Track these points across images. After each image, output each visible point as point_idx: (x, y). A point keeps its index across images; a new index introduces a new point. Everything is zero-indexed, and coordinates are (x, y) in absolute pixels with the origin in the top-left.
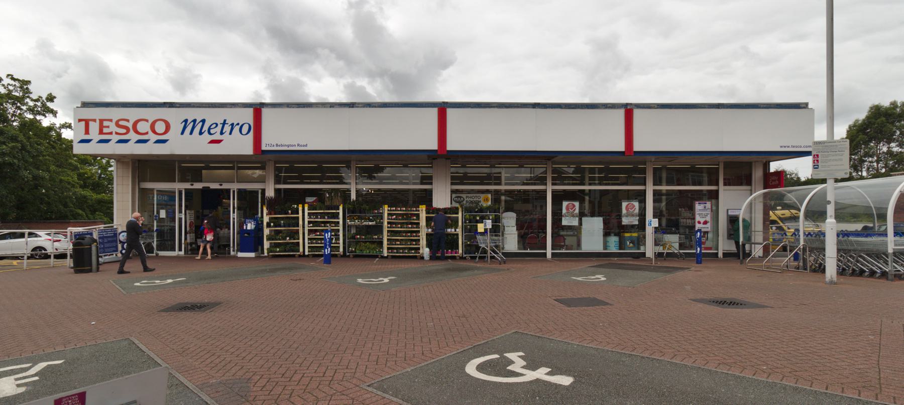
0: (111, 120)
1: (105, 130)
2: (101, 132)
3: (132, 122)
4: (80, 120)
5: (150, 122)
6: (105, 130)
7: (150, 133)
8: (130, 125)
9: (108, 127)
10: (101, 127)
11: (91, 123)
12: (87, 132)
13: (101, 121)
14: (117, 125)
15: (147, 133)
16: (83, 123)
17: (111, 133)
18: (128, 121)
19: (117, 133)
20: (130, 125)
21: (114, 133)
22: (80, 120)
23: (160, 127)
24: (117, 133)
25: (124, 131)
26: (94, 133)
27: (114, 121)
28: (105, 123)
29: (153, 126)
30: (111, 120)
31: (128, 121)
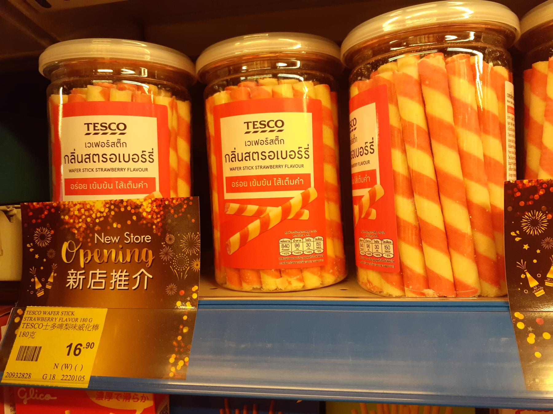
0: (257, 122)
1: (256, 127)
2: (254, 128)
3: (267, 122)
4: (245, 123)
5: (275, 121)
6: (256, 127)
7: (275, 127)
8: (266, 123)
9: (256, 125)
10: (254, 125)
11: (249, 123)
12: (248, 128)
13: (254, 122)
14: (260, 124)
15: (273, 127)
16: (246, 124)
17: (258, 128)
18: (265, 121)
19: (260, 128)
20: (266, 123)
21: (259, 127)
22: (245, 123)
23: (280, 124)
24: (260, 128)
25: (263, 126)
26: (251, 129)
27: (259, 122)
28: (256, 123)
29: (276, 123)
30: (257, 122)
31: (265, 121)
